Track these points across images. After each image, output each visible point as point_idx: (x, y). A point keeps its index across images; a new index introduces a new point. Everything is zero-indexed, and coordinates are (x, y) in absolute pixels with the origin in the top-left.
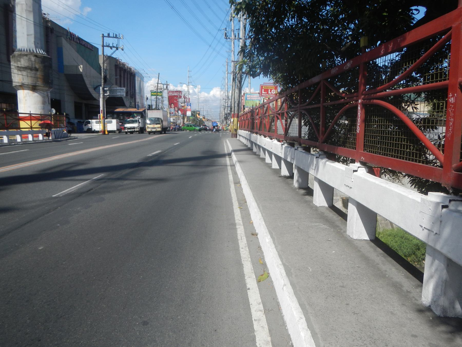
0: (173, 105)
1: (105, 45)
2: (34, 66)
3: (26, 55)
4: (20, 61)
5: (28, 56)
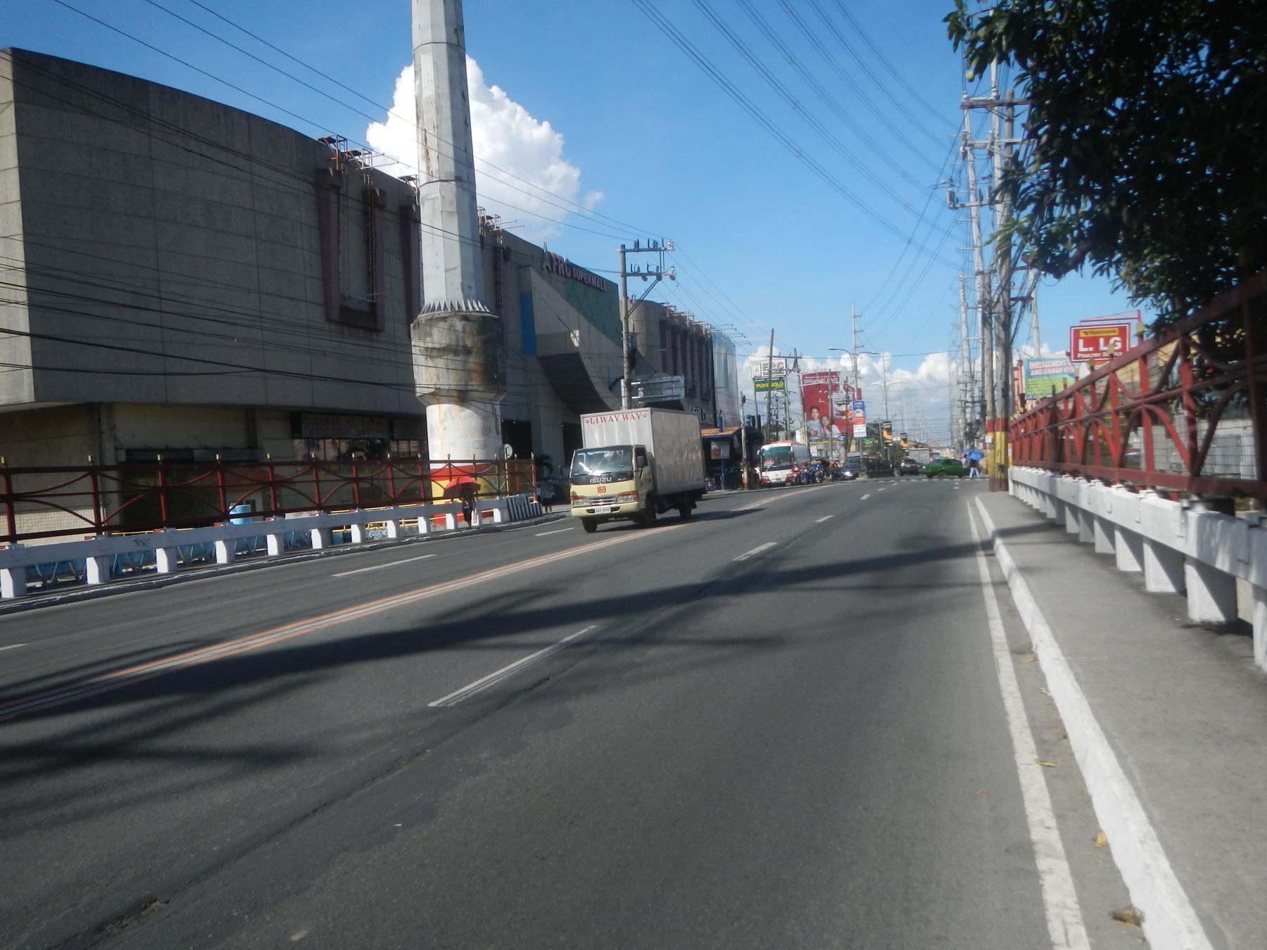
0: (815, 413)
1: (628, 270)
2: (461, 343)
3: (444, 319)
5: (449, 320)
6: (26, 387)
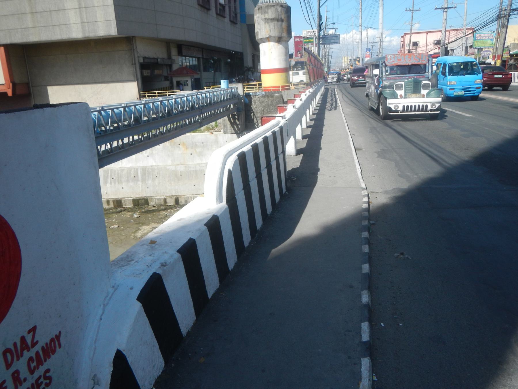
3: (274, 6)
4: (267, 13)
5: (275, 7)
6: (113, 28)
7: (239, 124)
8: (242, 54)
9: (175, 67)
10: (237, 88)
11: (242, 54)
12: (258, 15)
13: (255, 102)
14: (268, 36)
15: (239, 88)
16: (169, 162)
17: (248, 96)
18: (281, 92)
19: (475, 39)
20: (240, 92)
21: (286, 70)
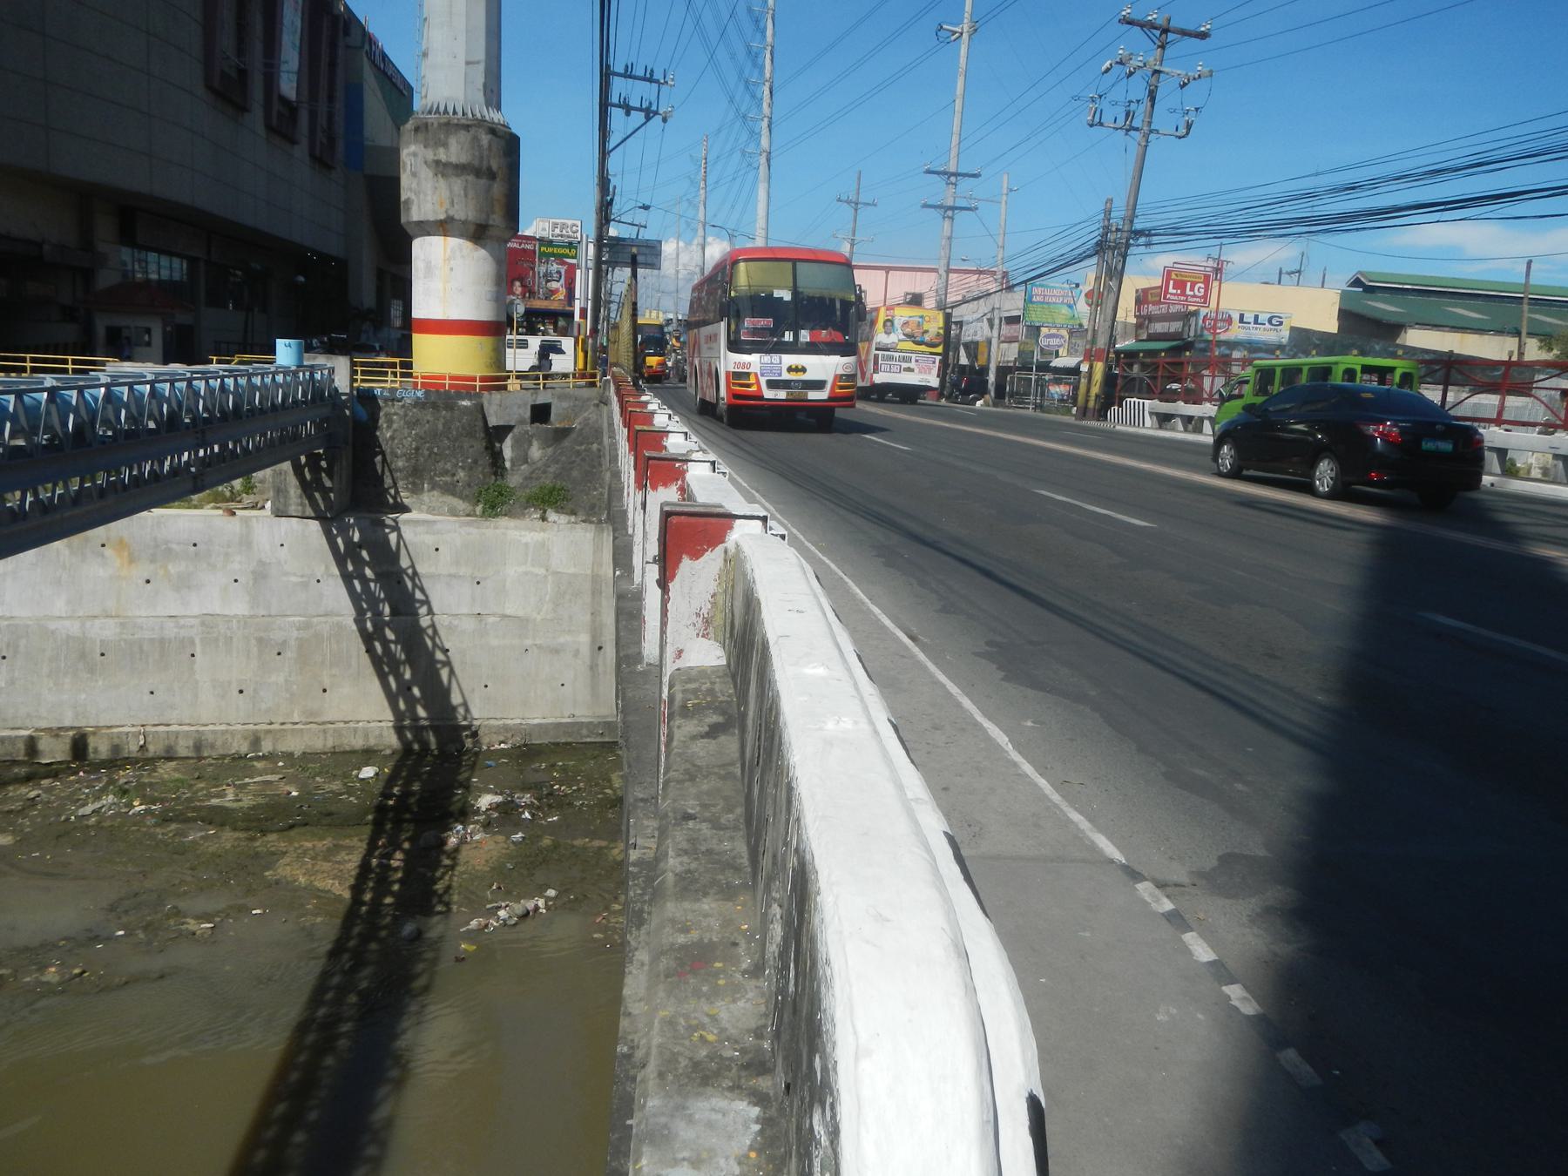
3: (467, 127)
4: (445, 145)
5: (473, 131)
7: (331, 490)
8: (342, 264)
9: (106, 279)
10: (332, 371)
11: (342, 264)
12: (413, 148)
13: (390, 422)
14: (442, 217)
15: (340, 373)
16: (60, 606)
17: (366, 399)
18: (479, 396)
19: (1028, 300)
20: (342, 382)
21: (494, 330)
